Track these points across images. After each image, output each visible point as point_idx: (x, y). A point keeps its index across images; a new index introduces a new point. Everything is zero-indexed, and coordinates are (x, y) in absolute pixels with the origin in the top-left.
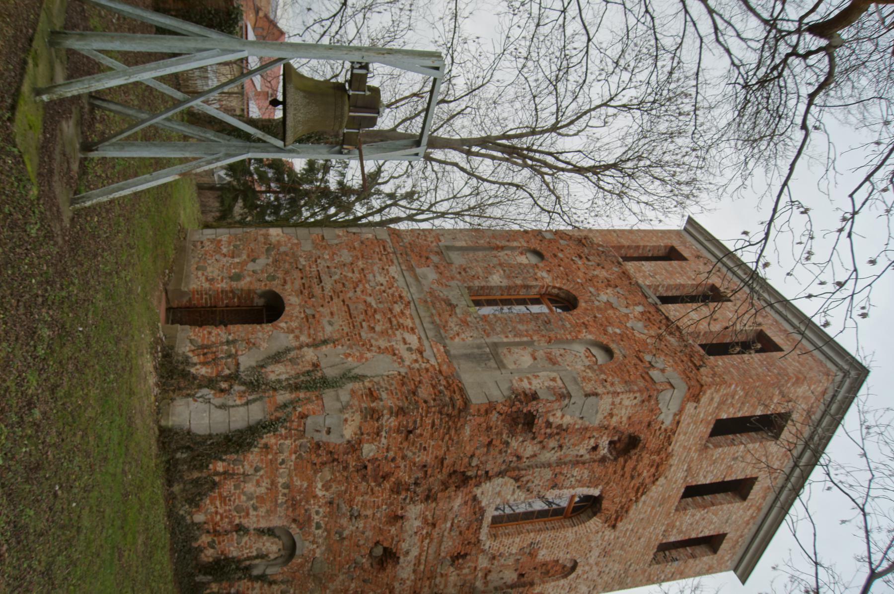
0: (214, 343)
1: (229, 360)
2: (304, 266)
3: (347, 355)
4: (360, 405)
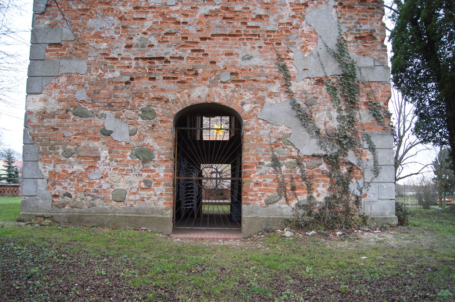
0: (276, 179)
1: (305, 164)
2: (122, 74)
3: (304, 48)
4: (379, 51)
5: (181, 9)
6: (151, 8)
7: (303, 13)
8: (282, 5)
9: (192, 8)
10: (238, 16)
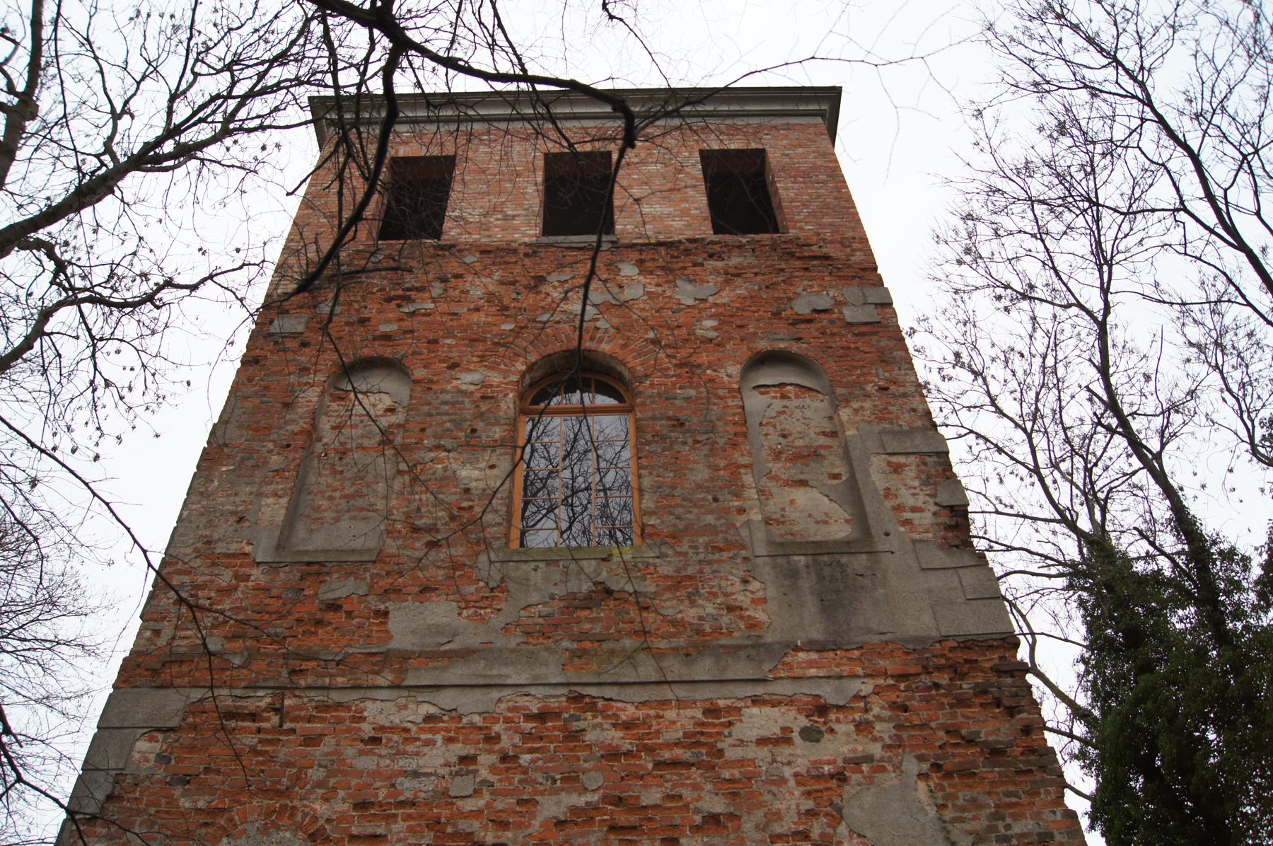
5: (488, 805)
6: (402, 804)
7: (837, 800)
8: (773, 782)
9: (521, 802)
10: (650, 819)
